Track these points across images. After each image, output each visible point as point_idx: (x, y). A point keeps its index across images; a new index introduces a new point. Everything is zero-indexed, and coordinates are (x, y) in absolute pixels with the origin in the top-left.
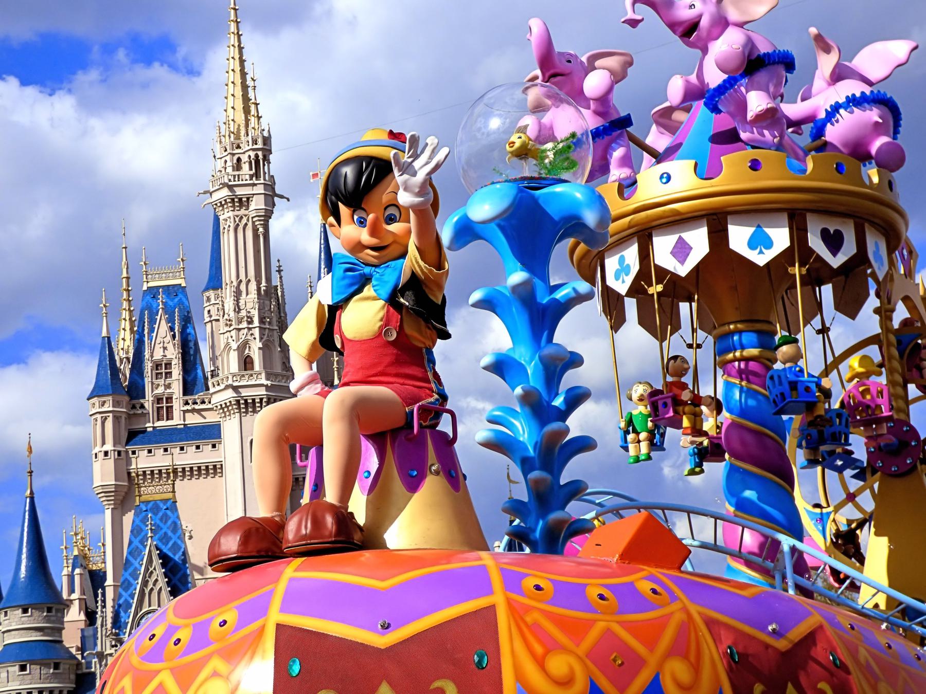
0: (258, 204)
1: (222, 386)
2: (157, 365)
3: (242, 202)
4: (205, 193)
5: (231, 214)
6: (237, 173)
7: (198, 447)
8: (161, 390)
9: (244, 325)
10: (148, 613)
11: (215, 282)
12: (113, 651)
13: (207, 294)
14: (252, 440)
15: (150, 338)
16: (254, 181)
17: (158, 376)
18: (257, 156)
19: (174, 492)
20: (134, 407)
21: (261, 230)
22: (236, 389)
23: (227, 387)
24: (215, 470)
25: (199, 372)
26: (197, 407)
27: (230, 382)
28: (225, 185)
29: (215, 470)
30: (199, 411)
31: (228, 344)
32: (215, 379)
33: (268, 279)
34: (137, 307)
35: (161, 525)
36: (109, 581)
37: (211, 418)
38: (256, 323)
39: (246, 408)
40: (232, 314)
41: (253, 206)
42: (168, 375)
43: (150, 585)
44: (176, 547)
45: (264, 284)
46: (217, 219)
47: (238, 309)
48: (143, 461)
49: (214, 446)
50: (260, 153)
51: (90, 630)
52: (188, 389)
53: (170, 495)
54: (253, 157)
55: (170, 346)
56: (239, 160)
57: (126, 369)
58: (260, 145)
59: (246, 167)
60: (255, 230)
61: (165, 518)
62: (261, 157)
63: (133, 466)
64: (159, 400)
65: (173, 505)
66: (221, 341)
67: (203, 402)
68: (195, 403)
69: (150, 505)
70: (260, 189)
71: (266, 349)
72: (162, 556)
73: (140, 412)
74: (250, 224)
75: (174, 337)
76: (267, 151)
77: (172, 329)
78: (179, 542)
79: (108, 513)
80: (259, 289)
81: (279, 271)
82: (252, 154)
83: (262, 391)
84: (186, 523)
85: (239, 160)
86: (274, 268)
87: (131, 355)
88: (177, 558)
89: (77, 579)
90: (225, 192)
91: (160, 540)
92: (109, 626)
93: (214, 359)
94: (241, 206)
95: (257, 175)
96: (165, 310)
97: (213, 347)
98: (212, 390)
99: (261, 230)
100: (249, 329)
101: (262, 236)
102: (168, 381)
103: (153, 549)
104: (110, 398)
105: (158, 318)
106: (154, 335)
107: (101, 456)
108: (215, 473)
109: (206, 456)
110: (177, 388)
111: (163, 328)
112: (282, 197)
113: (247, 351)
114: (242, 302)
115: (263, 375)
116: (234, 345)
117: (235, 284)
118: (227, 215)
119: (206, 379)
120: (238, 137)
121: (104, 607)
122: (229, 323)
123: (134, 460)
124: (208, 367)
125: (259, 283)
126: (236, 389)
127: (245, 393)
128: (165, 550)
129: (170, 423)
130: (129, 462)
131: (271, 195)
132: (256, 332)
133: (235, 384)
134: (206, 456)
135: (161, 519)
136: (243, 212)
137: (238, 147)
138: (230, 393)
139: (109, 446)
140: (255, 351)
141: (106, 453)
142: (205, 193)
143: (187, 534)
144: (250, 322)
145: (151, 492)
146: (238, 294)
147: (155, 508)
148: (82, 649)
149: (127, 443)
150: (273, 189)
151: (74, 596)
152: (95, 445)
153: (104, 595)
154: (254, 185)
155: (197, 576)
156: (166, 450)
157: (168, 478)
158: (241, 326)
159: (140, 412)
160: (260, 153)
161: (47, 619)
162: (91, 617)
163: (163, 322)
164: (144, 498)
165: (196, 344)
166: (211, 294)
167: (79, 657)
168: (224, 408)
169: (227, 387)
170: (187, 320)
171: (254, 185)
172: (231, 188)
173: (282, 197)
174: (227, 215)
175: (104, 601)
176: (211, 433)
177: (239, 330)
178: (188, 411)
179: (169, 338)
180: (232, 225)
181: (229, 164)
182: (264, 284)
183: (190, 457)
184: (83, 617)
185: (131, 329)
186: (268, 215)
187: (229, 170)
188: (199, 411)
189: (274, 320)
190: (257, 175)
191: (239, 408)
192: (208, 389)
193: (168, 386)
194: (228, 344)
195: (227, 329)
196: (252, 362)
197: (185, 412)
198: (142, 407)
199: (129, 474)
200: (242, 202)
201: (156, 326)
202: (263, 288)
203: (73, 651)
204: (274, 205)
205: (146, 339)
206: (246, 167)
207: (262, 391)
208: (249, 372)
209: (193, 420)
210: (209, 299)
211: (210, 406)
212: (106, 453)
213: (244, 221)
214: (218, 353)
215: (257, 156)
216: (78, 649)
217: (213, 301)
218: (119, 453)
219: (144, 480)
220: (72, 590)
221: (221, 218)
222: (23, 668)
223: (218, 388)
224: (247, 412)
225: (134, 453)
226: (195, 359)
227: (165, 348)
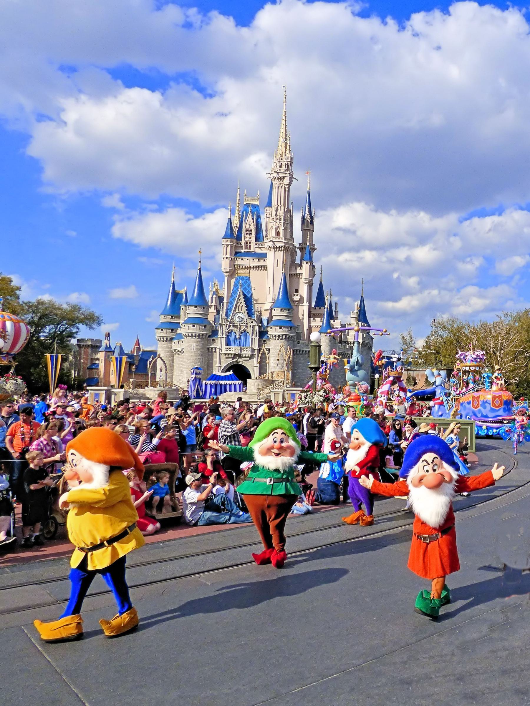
0: (287, 180)
1: (269, 241)
2: (247, 231)
3: (282, 179)
4: (269, 173)
5: (277, 182)
6: (280, 168)
7: (259, 260)
8: (247, 239)
9: (278, 221)
10: (238, 312)
11: (269, 205)
12: (225, 324)
13: (266, 208)
14: (278, 260)
15: (245, 221)
16: (286, 172)
17: (247, 234)
18: (288, 163)
19: (249, 274)
20: (238, 244)
21: (287, 189)
22: (273, 242)
23: (271, 241)
24: (264, 268)
25: (261, 235)
26: (259, 246)
27: (272, 239)
28: (276, 172)
29: (264, 268)
30: (260, 248)
31: (272, 226)
32: (266, 238)
33: (288, 206)
34: (241, 209)
35: (244, 284)
36: (225, 300)
37: (264, 251)
38: (282, 220)
39: (277, 249)
40: (274, 217)
41: (285, 180)
42: (251, 234)
43: (239, 304)
44: (249, 292)
45: (286, 208)
46: (272, 183)
47: (276, 215)
48: (240, 262)
49: (264, 260)
50: (289, 163)
51: (217, 316)
52: (257, 240)
53: (248, 275)
54: (286, 164)
55: (252, 225)
56: (281, 164)
57: (236, 230)
58: (289, 160)
59: (283, 167)
60: (285, 189)
61: (245, 282)
62: (289, 164)
63: (236, 264)
64: (247, 242)
65: (249, 279)
66: (270, 225)
67: (262, 245)
68: (259, 245)
69: (241, 277)
70: (288, 175)
71: (285, 230)
72: (244, 294)
73: (240, 245)
74: (283, 187)
75: (253, 221)
76: (291, 163)
77: (253, 219)
78: (250, 291)
79: (226, 279)
80: (284, 209)
81: (292, 204)
82: (286, 163)
83: (283, 244)
84: (253, 285)
85: (281, 164)
86: (290, 202)
87: (238, 226)
88: (249, 296)
89: (214, 299)
90: (276, 174)
91: (244, 289)
92: (224, 315)
93: (267, 231)
94: (281, 180)
95: (287, 170)
96: (252, 212)
97: (267, 227)
98: (265, 241)
99: (287, 189)
100: (280, 222)
101: (287, 192)
102: (250, 236)
103: (241, 292)
104: (230, 240)
105: (249, 214)
106: (247, 220)
107: (225, 259)
108: (264, 269)
109: (261, 263)
110: (253, 239)
111: (250, 218)
112: (295, 179)
113: (278, 230)
114: (278, 213)
115: (283, 239)
116: (274, 227)
117: (276, 206)
118: (275, 182)
119: (263, 237)
120: (282, 156)
121: (223, 309)
122: (273, 219)
123: (236, 262)
124: (265, 233)
125: (285, 207)
126: (273, 242)
127: (276, 243)
128: (245, 293)
129: (250, 250)
130: (235, 262)
131: (291, 178)
132: (282, 224)
133: (273, 240)
134: (261, 263)
135: (244, 283)
136: (281, 182)
137: (282, 159)
138: (271, 243)
139: (228, 256)
140: (281, 230)
141: (227, 258)
142: (269, 173)
143: (253, 289)
144: (280, 220)
145: (241, 273)
146: (277, 210)
147: (243, 279)
148: (214, 322)
149: (235, 255)
150: (293, 176)
151: (212, 304)
152: (223, 255)
153: (223, 305)
154: (286, 173)
155: (255, 302)
156: (248, 259)
157: (248, 269)
158: (277, 221)
159: (240, 245)
160: (289, 163)
161: (203, 311)
162: (218, 312)
163: (250, 216)
164: (239, 275)
165: (261, 225)
166: (268, 208)
167: (213, 324)
168: (269, 248)
169: (271, 241)
170: (258, 217)
171: (286, 173)
172: (278, 173)
173: (295, 179)
174: (275, 182)
175: (223, 307)
176: (264, 256)
177: (276, 222)
178: (256, 247)
179: (252, 222)
180: (277, 186)
181: (278, 165)
182: (286, 208)
183: (256, 263)
184: (215, 311)
185: (239, 217)
186: (290, 184)
187: (278, 167)
188: (260, 248)
189: (289, 220)
190: (287, 170)
191: (274, 249)
192: (264, 241)
193: (250, 238)
194: (272, 226)
195: (272, 221)
196: (280, 234)
197: (255, 247)
198: (241, 244)
199: (234, 266)
200: (282, 179)
201: (248, 217)
202: (286, 209)
203: (211, 322)
204: (292, 181)
205: (244, 221)
206: (283, 167)
207: (283, 244)
208: (279, 237)
209: (258, 250)
210: (266, 210)
211: (264, 247)
212: (227, 258)
213: (281, 185)
214: (268, 229)
215: (288, 163)
216: (213, 322)
217: (268, 211)
218: (231, 258)
219: (240, 269)
220: (212, 302)
221: (273, 183)
222: (194, 326)
223: (267, 241)
224: (276, 250)
225: (236, 259)
226: (260, 230)
227: (250, 225)
